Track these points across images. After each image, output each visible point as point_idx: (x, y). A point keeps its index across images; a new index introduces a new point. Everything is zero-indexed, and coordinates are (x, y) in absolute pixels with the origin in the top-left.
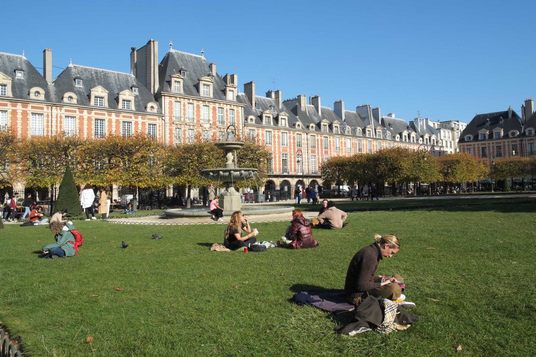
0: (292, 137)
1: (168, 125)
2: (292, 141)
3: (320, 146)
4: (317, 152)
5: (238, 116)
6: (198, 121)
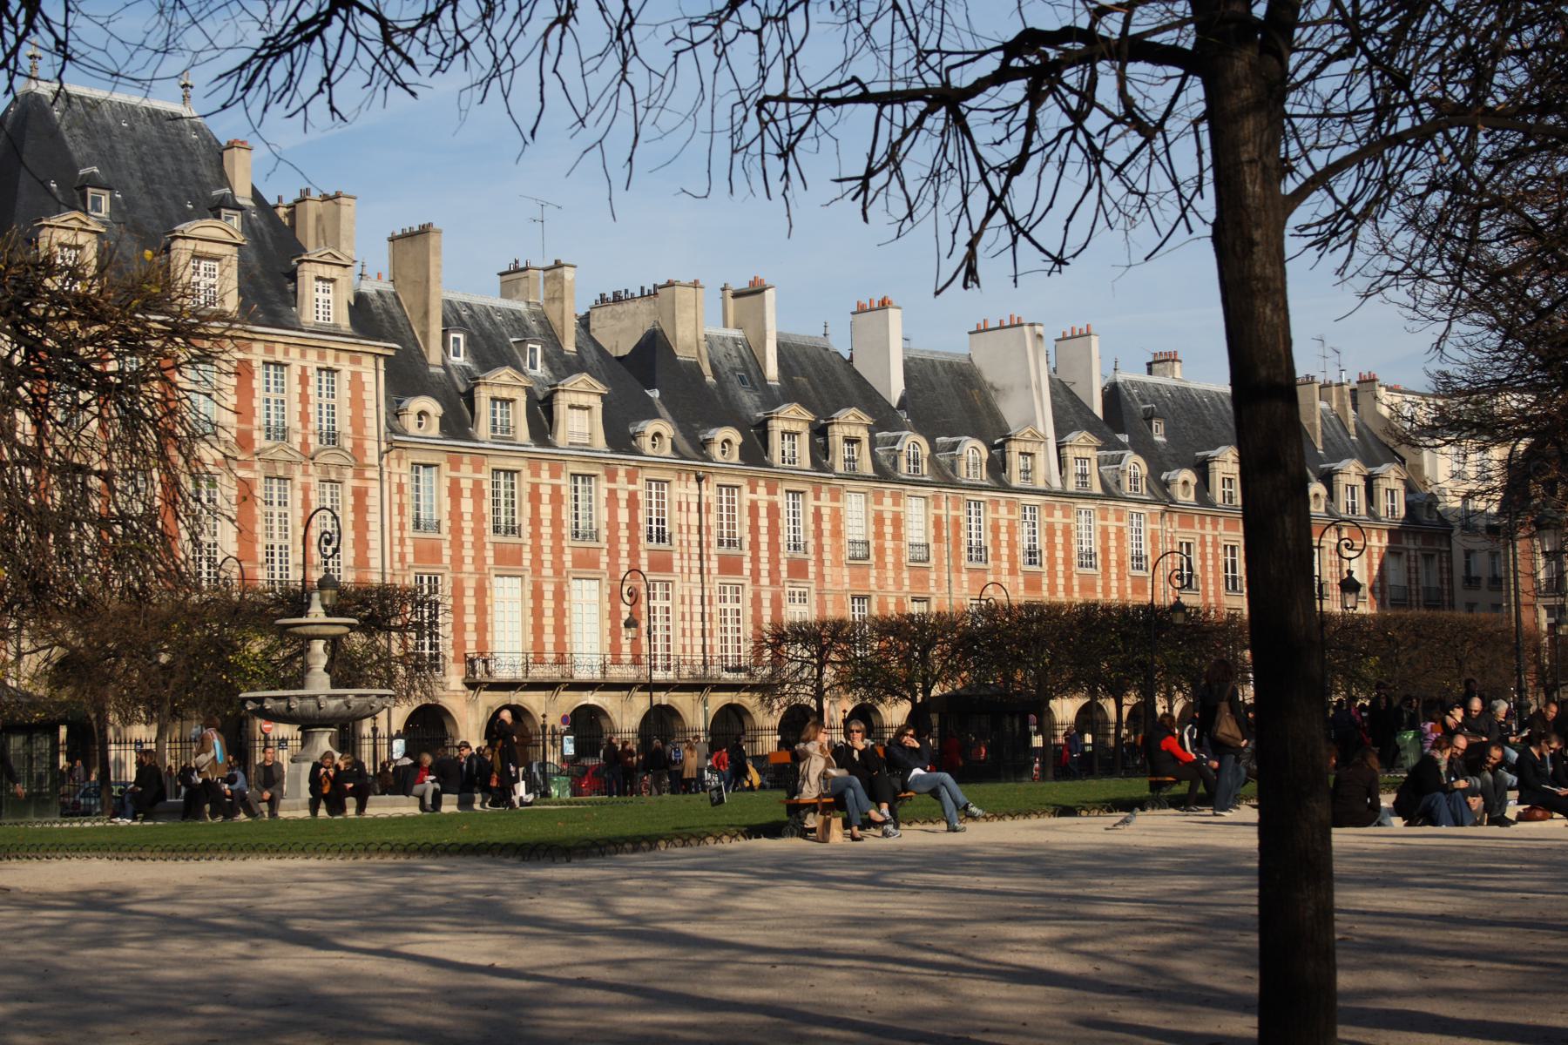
0: (623, 496)
2: (623, 516)
3: (764, 539)
4: (747, 566)
5: (357, 402)
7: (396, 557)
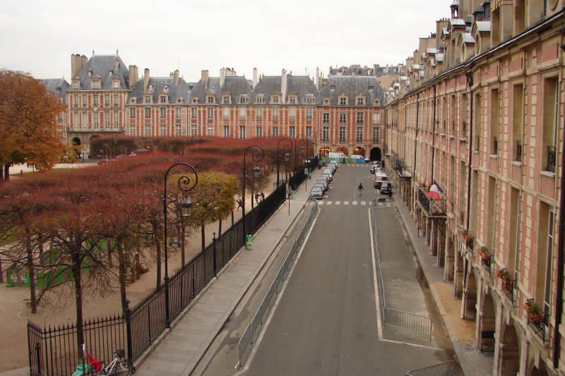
3: (202, 116)
4: (198, 121)
6: (90, 106)
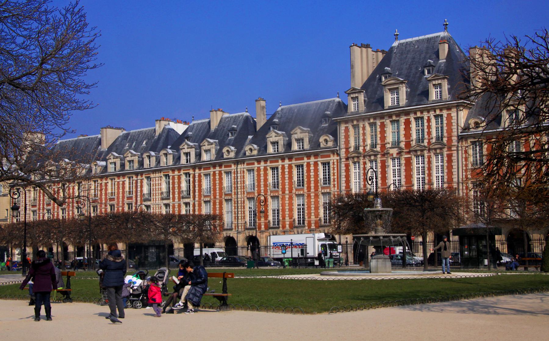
1: (343, 160)
7: (464, 176)
